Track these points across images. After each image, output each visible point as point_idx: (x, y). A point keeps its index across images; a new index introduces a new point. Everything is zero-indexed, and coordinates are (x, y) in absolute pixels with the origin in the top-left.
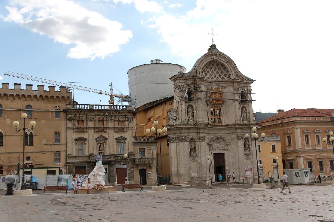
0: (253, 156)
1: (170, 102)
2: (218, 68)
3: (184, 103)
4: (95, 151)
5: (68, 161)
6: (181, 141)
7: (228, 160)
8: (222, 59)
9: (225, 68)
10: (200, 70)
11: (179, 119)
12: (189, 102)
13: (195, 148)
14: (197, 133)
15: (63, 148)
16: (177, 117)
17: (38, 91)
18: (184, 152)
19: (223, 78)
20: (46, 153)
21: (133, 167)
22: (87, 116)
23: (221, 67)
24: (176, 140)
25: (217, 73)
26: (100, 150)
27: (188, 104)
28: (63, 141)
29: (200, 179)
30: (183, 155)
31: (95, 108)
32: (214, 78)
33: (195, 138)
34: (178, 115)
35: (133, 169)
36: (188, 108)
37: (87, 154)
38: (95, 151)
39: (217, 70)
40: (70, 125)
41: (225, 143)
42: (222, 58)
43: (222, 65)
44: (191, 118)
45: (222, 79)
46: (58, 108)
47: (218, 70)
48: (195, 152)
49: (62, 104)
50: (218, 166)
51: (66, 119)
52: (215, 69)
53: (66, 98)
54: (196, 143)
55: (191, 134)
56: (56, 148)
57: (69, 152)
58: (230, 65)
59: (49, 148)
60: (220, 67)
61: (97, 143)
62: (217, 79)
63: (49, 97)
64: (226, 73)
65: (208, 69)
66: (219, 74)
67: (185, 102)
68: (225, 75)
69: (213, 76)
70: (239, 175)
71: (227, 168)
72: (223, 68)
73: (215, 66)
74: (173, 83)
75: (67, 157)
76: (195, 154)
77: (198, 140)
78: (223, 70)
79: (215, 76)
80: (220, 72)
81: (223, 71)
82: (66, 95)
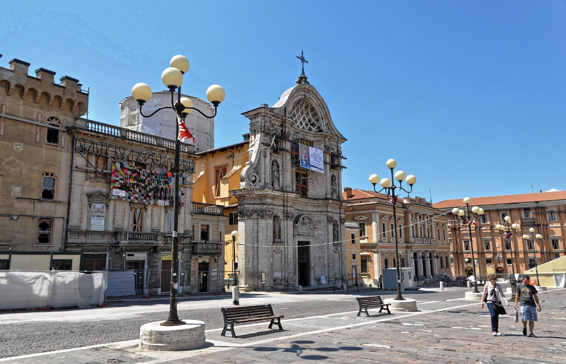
1: (229, 154)
3: (268, 155)
4: (126, 223)
5: (69, 241)
6: (262, 217)
7: (314, 253)
8: (314, 100)
9: (315, 114)
10: (290, 109)
12: (274, 154)
13: (280, 231)
14: (284, 206)
15: (60, 211)
16: (257, 177)
17: (12, 74)
19: (310, 129)
20: (20, 217)
21: (191, 258)
22: (118, 150)
23: (310, 112)
24: (251, 215)
25: (304, 119)
26: (135, 223)
28: (61, 195)
30: (265, 241)
33: (280, 214)
34: (258, 174)
36: (273, 165)
37: (110, 229)
38: (126, 223)
40: (79, 161)
43: (313, 109)
45: (309, 130)
46: (54, 122)
48: (280, 238)
49: (64, 115)
51: (70, 148)
52: (302, 114)
53: (76, 104)
54: (282, 223)
55: (276, 207)
56: (45, 209)
57: (73, 222)
59: (27, 207)
60: (308, 112)
62: (303, 128)
63: (40, 91)
64: (315, 122)
65: (295, 111)
67: (271, 154)
68: (313, 125)
69: (298, 123)
73: (303, 108)
75: (67, 232)
76: (279, 240)
78: (311, 117)
79: (301, 124)
80: (307, 119)
81: (312, 118)
82: (76, 98)
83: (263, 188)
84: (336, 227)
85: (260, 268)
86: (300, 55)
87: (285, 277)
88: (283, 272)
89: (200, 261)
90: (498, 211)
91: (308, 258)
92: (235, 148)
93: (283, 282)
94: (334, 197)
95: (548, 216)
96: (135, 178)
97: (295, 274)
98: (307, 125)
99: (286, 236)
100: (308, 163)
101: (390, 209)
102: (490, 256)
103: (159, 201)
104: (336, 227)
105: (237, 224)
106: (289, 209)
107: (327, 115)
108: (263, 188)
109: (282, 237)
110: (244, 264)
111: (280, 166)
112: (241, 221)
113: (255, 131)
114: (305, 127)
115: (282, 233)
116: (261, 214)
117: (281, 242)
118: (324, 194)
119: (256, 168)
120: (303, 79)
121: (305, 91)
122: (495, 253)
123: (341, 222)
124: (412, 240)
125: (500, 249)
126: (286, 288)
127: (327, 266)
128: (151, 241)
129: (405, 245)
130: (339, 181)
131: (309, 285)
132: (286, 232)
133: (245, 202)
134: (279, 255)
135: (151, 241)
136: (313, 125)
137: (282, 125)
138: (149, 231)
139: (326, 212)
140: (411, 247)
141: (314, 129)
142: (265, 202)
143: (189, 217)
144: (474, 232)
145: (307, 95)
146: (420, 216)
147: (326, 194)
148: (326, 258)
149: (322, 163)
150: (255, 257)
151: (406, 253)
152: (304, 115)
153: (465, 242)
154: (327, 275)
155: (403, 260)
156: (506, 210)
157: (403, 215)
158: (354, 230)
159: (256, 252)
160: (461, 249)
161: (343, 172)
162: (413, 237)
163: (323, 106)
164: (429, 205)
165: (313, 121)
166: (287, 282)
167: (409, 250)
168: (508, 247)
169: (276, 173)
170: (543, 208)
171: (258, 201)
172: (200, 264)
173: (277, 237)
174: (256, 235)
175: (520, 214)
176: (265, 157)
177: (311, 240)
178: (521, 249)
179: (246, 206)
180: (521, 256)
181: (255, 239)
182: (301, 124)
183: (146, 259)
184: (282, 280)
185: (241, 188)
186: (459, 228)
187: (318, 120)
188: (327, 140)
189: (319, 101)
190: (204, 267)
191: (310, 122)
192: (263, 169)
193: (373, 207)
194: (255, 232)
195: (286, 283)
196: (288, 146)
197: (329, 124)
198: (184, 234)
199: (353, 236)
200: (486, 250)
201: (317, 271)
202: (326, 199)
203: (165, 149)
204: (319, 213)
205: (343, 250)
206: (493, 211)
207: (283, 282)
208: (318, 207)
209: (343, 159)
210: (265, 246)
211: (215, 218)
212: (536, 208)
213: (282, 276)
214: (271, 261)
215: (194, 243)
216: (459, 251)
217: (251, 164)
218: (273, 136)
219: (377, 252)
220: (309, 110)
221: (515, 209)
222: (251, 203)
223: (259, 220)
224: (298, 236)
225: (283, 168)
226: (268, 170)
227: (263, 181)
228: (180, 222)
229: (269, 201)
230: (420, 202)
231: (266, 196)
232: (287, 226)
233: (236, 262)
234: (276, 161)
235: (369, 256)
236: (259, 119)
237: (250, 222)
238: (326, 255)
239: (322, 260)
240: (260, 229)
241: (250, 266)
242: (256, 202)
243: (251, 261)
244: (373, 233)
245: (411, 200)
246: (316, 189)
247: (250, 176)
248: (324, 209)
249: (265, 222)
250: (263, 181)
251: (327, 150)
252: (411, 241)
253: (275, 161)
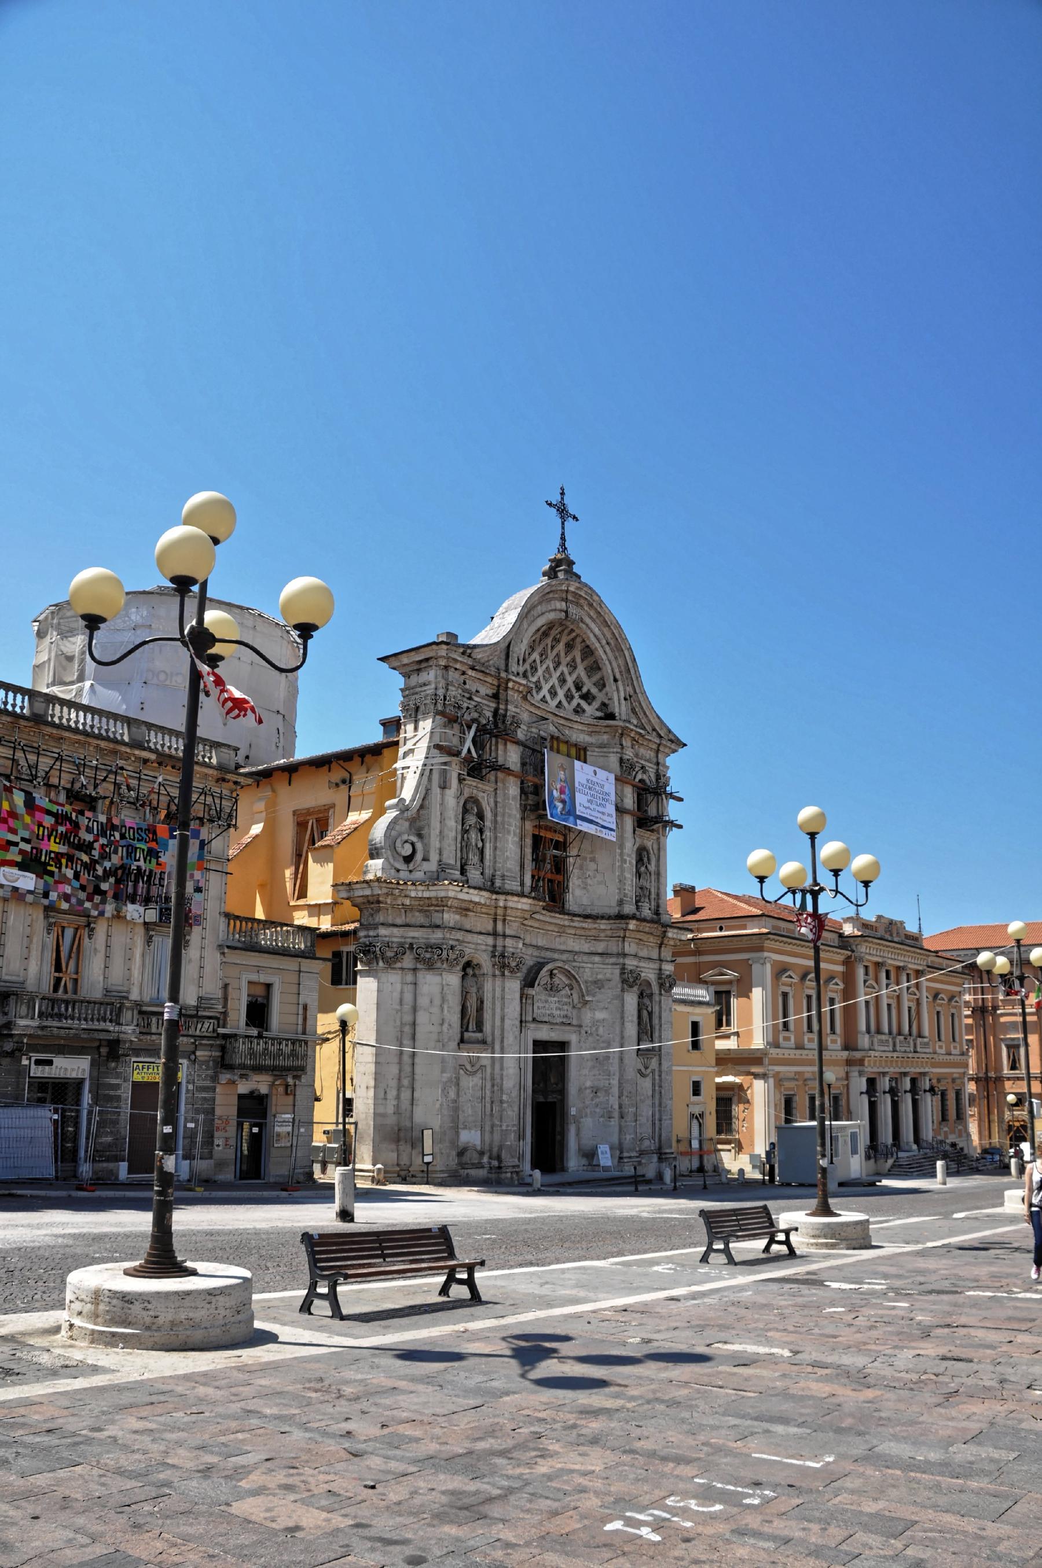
0: (660, 1064)
1: (338, 774)
2: (568, 659)
3: (454, 782)
4: (33, 968)
6: (430, 966)
7: (579, 1078)
8: (593, 625)
9: (594, 668)
10: (521, 648)
11: (425, 859)
12: (470, 781)
13: (480, 1009)
14: (495, 934)
16: (419, 846)
18: (442, 1024)
19: (578, 710)
21: (215, 1078)
22: (19, 755)
23: (578, 660)
24: (398, 957)
25: (562, 681)
26: (58, 968)
27: (467, 793)
29: (490, 1158)
30: (435, 1036)
31: (56, 720)
32: (548, 697)
34: (420, 836)
35: (214, 1089)
36: (465, 811)
38: (33, 968)
39: (563, 668)
41: (575, 996)
42: (594, 620)
43: (588, 652)
44: (474, 858)
47: (566, 671)
48: (479, 1028)
50: (541, 1099)
52: (558, 664)
54: (488, 986)
55: (469, 937)
58: (616, 658)
60: (574, 660)
61: (50, 924)
62: (559, 705)
64: (594, 691)
65: (535, 656)
66: (566, 688)
67: (461, 780)
68: (587, 697)
69: (545, 691)
70: (617, 1142)
71: (573, 1111)
72: (585, 662)
73: (561, 647)
74: (399, 681)
76: (479, 1035)
77: (497, 972)
79: (553, 693)
83: (435, 878)
84: (646, 1001)
85: (420, 1115)
86: (555, 499)
87: (491, 1145)
88: (487, 1128)
89: (243, 1088)
91: (562, 1092)
92: (357, 759)
93: (485, 1159)
94: (644, 912)
96: (64, 838)
97: (521, 1137)
98: (569, 697)
99: (498, 1023)
100: (570, 811)
101: (804, 951)
103: (130, 907)
104: (646, 1001)
105: (355, 983)
106: (509, 942)
107: (629, 672)
108: (435, 878)
109: (487, 1027)
110: (371, 1101)
111: (488, 815)
112: (367, 974)
113: (417, 709)
114: (565, 703)
115: (487, 1016)
116: (429, 957)
117: (484, 1042)
118: (614, 903)
119: (415, 820)
120: (561, 566)
121: (566, 600)
123: (661, 985)
124: (864, 1041)
126: (493, 1176)
127: (616, 1114)
128: (102, 1025)
129: (845, 1054)
130: (658, 866)
131: (563, 1169)
132: (498, 1011)
133: (380, 918)
134: (476, 1080)
135: (102, 1025)
136: (587, 697)
137: (496, 696)
138: (97, 995)
139: (618, 955)
140: (861, 1062)
141: (590, 710)
142: (438, 922)
143: (213, 958)
144: (1035, 1018)
145: (573, 610)
146: (888, 972)
147: (621, 903)
148: (615, 1090)
149: (611, 809)
150: (406, 1082)
151: (847, 1078)
152: (563, 668)
153: (1008, 1047)
154: (615, 1139)
155: (836, 1099)
157: (840, 968)
158: (698, 1010)
159: (407, 1069)
160: (999, 1068)
161: (673, 837)
162: (868, 1031)
163: (619, 645)
164: (913, 941)
165: (588, 686)
166: (499, 1158)
169: (473, 835)
171: (419, 918)
172: (241, 1097)
173: (472, 1026)
174: (408, 1018)
176: (444, 787)
177: (573, 1038)
179: (383, 931)
181: (407, 1029)
182: (553, 693)
183: (87, 1075)
184: (482, 1153)
185: (370, 877)
186: (995, 1008)
187: (601, 685)
188: (627, 742)
189: (606, 630)
190: (254, 1107)
191: (578, 688)
192: (435, 824)
193: (755, 944)
194: (407, 1007)
195: (495, 1163)
196: (512, 756)
197: (635, 698)
198: (197, 1008)
199: (695, 1026)
201: (586, 1128)
202: (620, 917)
203: (153, 757)
204: (597, 959)
205: (664, 1067)
207: (485, 1159)
208: (596, 939)
209: (671, 801)
210: (434, 1052)
211: (291, 964)
213: (482, 1141)
214: (452, 1095)
215: (225, 1036)
216: (992, 1074)
217: (403, 808)
218: (469, 727)
219: (764, 1076)
220: (577, 654)
222: (399, 921)
223: (420, 975)
224: (533, 1026)
225: (495, 822)
226: (453, 825)
227: (434, 857)
228: (189, 971)
229: (450, 918)
230: (888, 932)
231: (441, 904)
232: (504, 995)
233: (348, 1096)
234: (476, 802)
235: (740, 1086)
236: (430, 675)
237: (394, 978)
238: (615, 1082)
239: (601, 1097)
240: (423, 1001)
241: (390, 1110)
242: (413, 921)
243: (392, 1093)
244: (753, 1022)
245: (865, 925)
246: (594, 885)
247: (398, 844)
248: (614, 947)
249: (438, 979)
250: (434, 857)
251: (626, 771)
252: (860, 1045)
253: (473, 800)
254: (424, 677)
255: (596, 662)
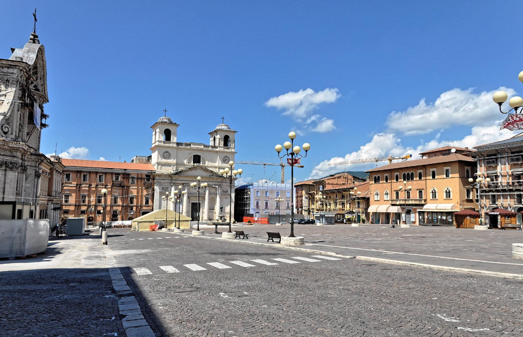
6: (11, 169)
16: (10, 129)
90: (97, 173)
95: (130, 180)
102: (84, 208)
122: (89, 206)
125: (93, 203)
144: (94, 189)
156: (103, 173)
157: (49, 171)
160: (62, 201)
167: (50, 203)
168: (99, 201)
170: (129, 174)
171: (8, 153)
175: (112, 178)
178: (109, 203)
180: (108, 208)
200: (82, 203)
206: (93, 172)
212: (123, 174)
221: (109, 173)
223: (7, 172)
227: (14, 133)
240: (7, 181)
242: (6, 154)
250: (14, 133)
254: (11, 70)
255: (37, 72)
